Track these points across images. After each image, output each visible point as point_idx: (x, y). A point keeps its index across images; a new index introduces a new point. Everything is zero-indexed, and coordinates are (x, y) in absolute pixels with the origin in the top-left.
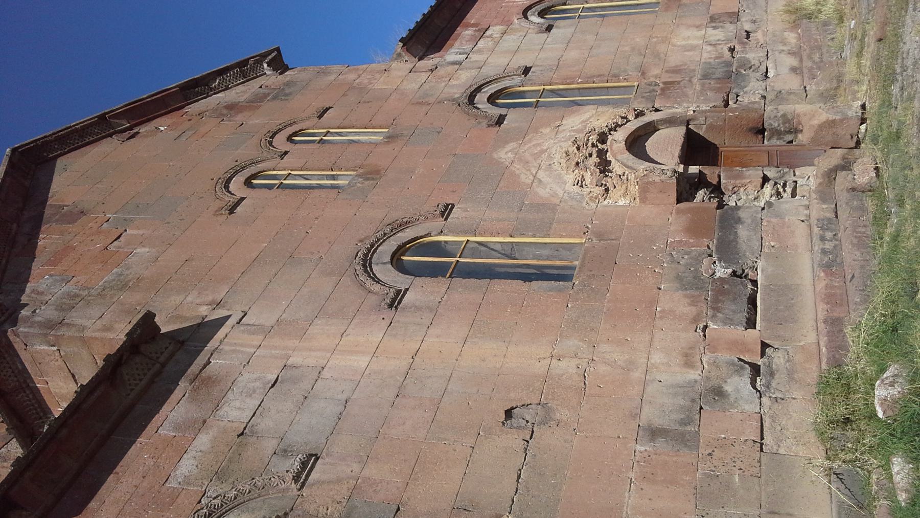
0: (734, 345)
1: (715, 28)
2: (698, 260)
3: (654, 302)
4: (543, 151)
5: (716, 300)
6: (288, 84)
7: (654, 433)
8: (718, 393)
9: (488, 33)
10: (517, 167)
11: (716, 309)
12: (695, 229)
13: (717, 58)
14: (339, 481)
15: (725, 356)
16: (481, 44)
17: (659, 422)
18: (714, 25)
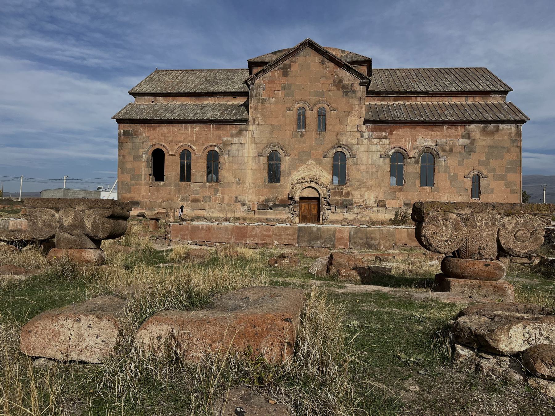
0: (254, 207)
1: (375, 202)
2: (273, 201)
3: (262, 196)
4: (311, 170)
5: (263, 205)
6: (354, 92)
7: (237, 198)
8: (244, 205)
9: (384, 140)
10: (305, 166)
11: (261, 205)
12: (282, 201)
13: (355, 203)
14: (225, 160)
15: (251, 206)
16: (378, 140)
17: (238, 198)
18: (377, 201)
